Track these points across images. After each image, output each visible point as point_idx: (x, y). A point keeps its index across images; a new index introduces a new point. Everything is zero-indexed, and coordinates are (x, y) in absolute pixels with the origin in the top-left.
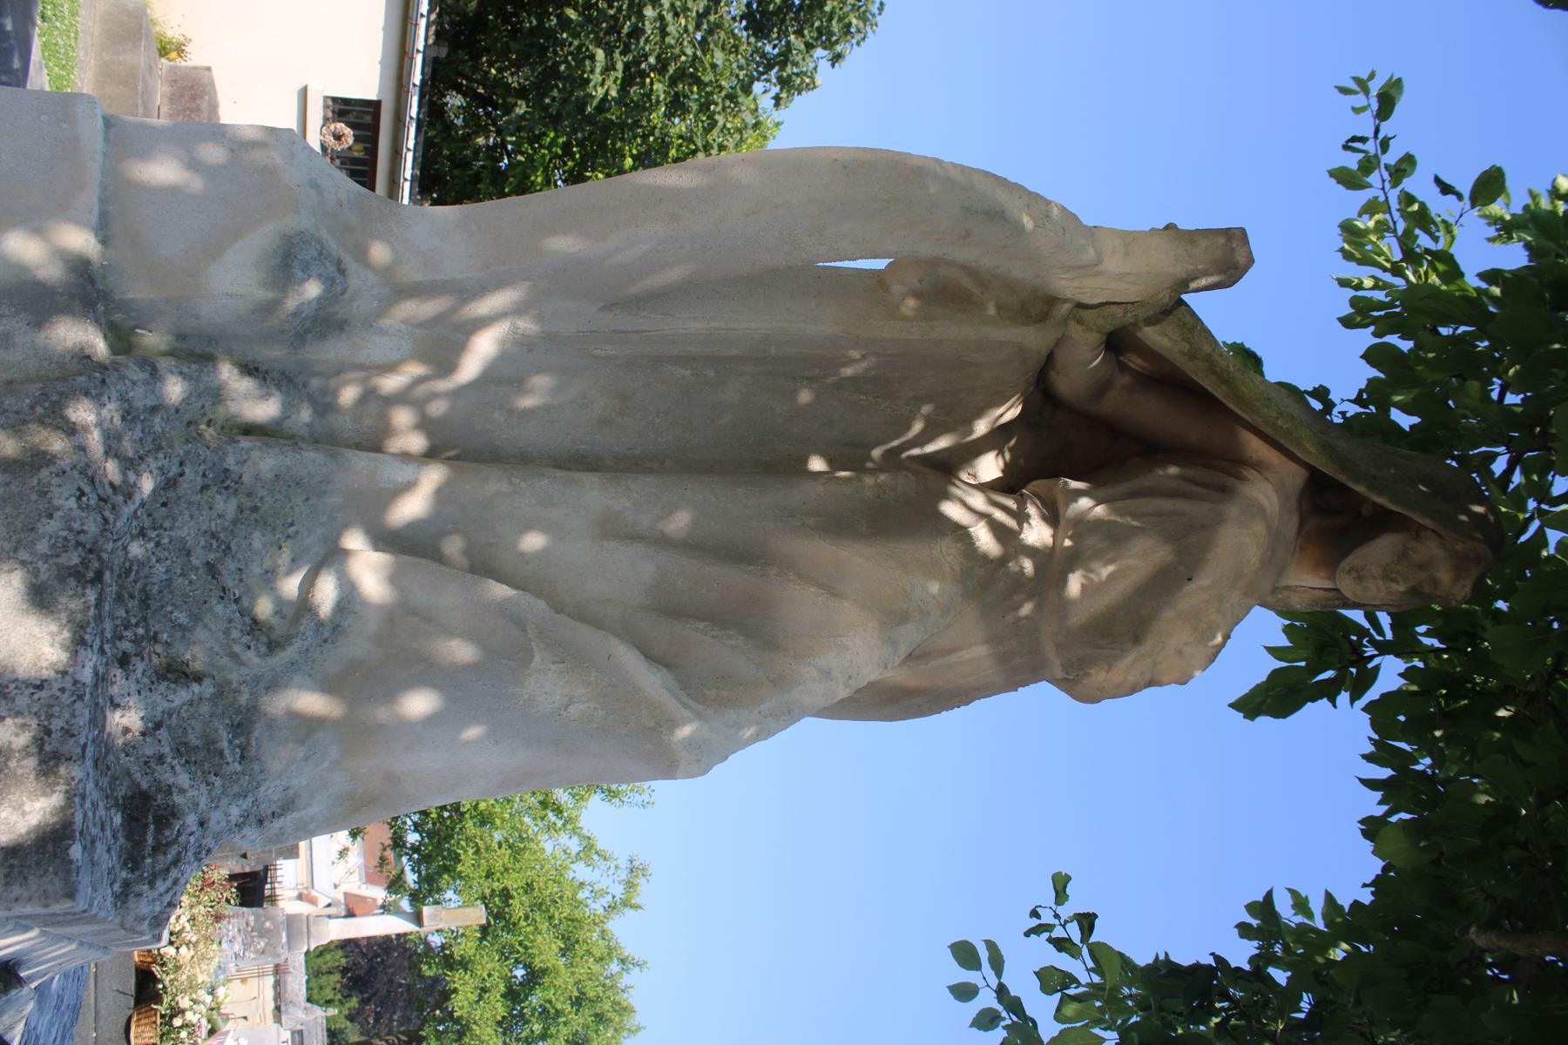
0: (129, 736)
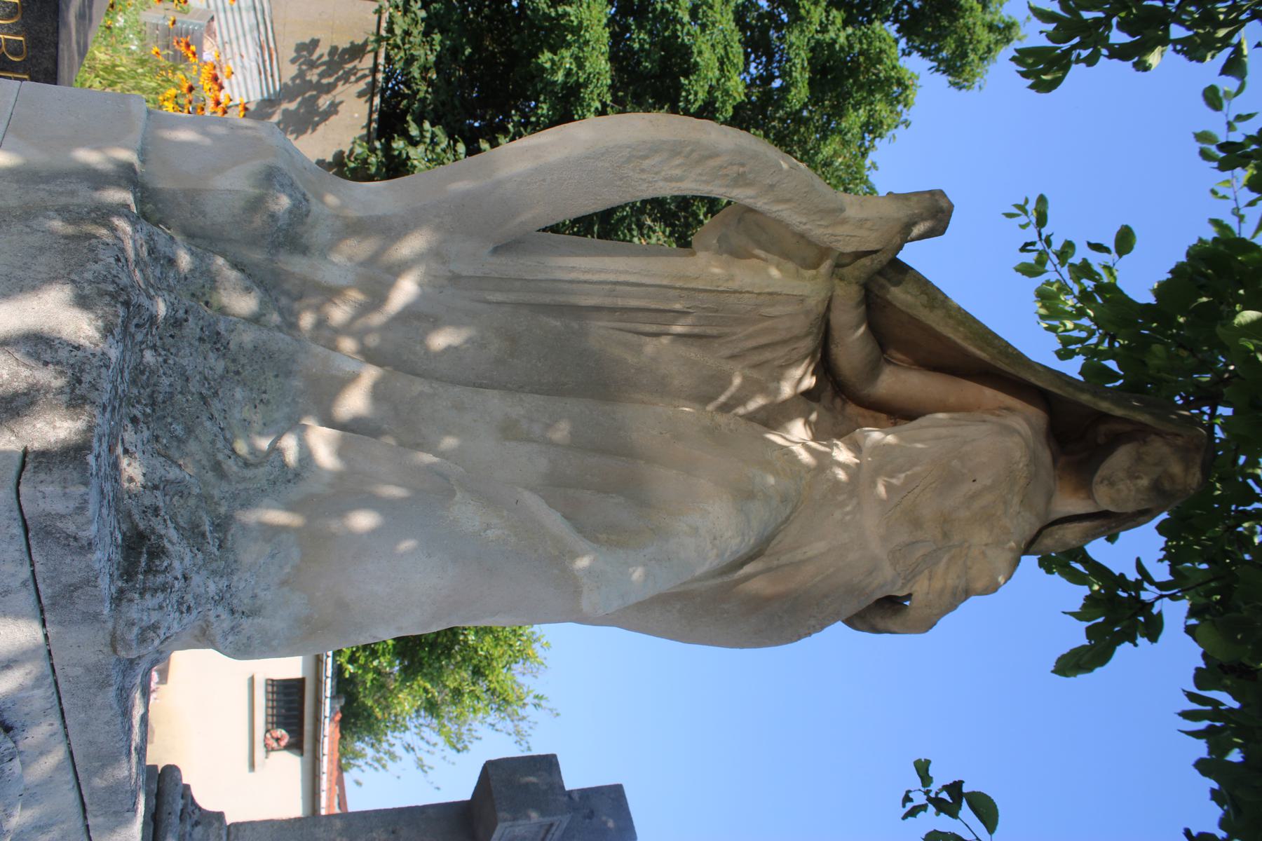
0: (132, 485)
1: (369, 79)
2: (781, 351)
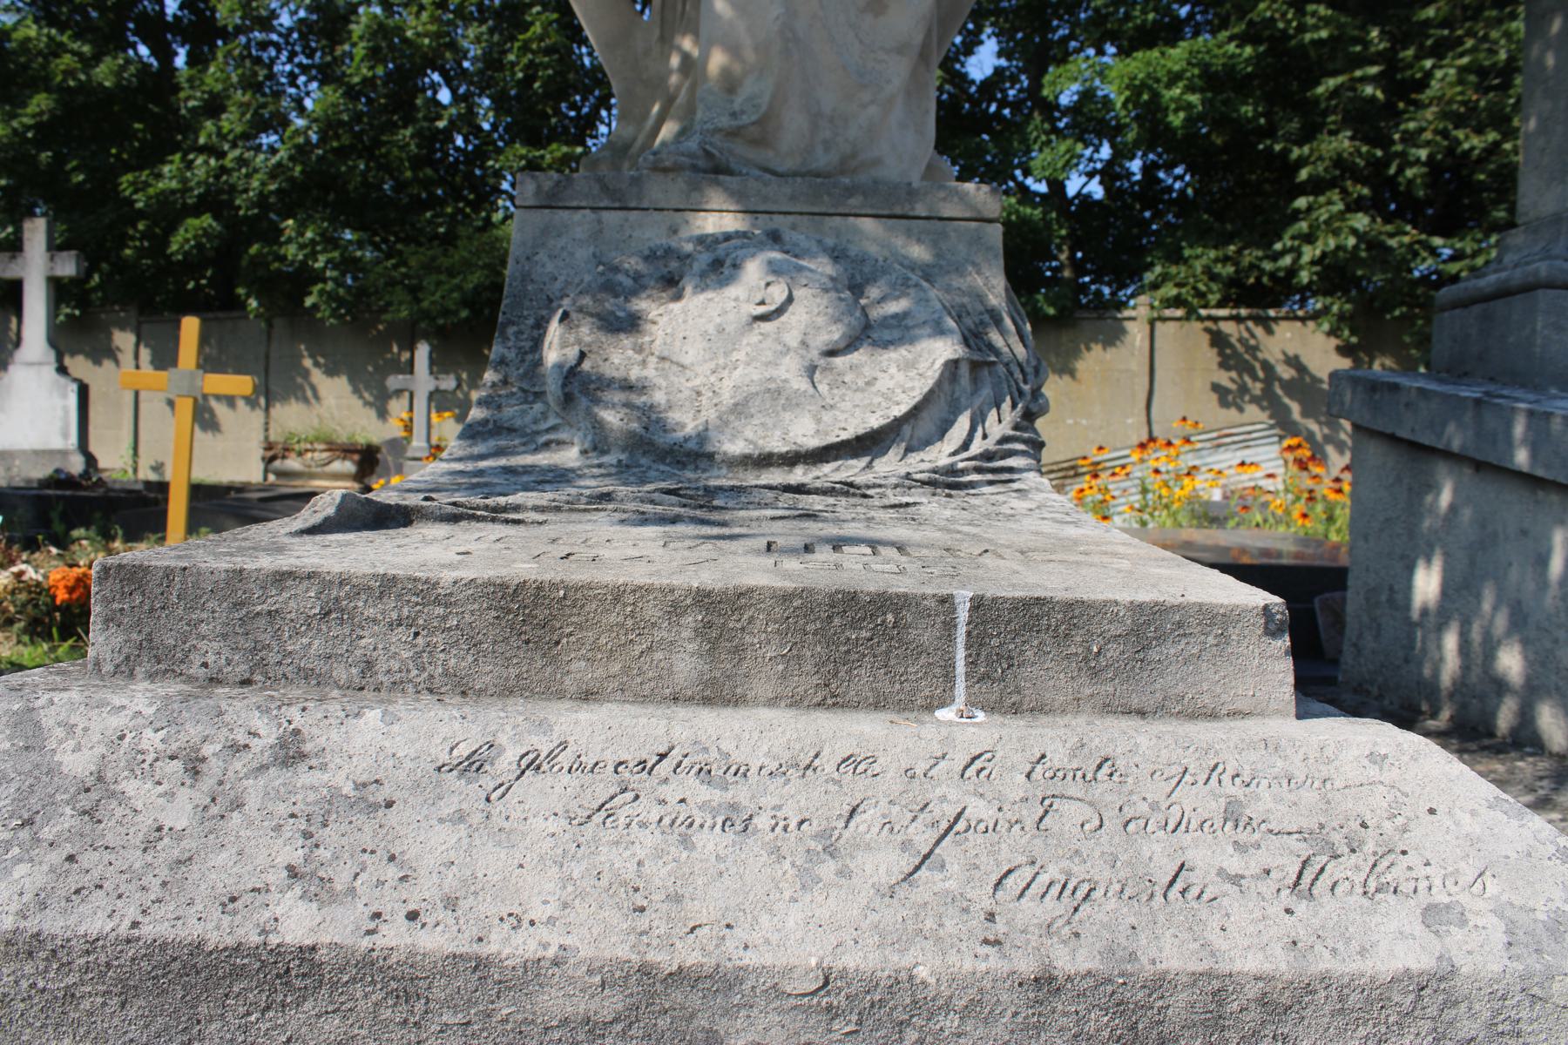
1: (1250, 324)
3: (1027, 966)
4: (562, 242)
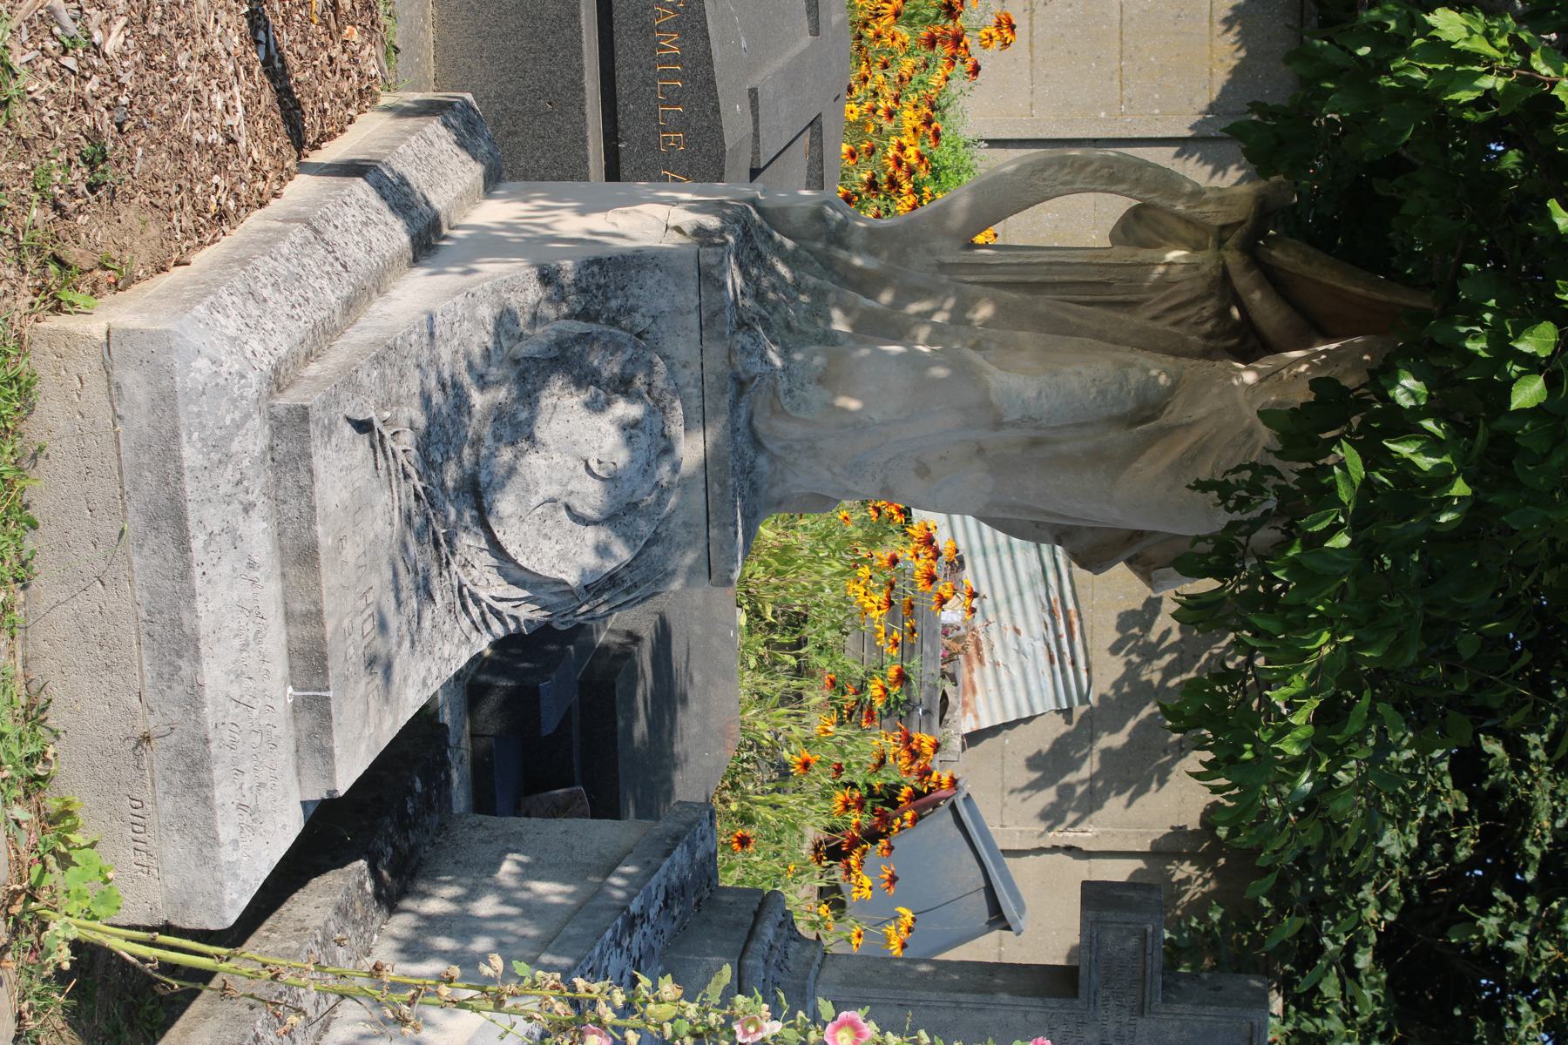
2: (1192, 311)
3: (210, 736)
4: (672, 288)
